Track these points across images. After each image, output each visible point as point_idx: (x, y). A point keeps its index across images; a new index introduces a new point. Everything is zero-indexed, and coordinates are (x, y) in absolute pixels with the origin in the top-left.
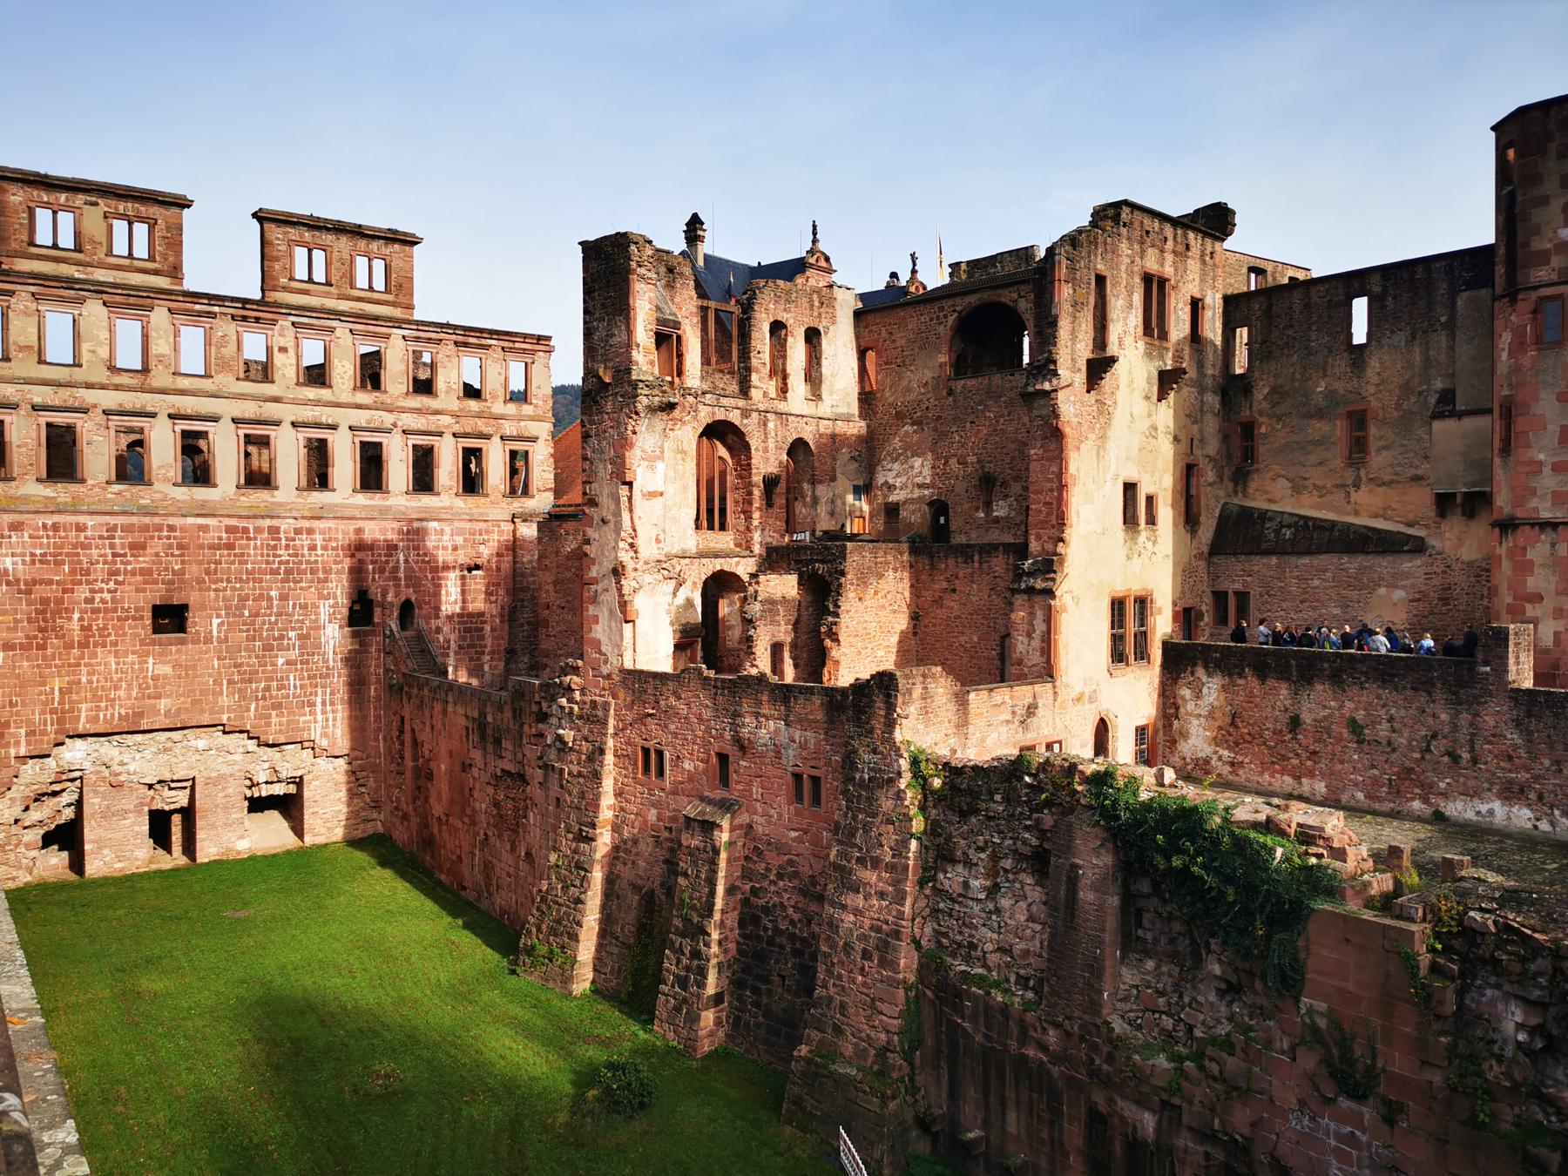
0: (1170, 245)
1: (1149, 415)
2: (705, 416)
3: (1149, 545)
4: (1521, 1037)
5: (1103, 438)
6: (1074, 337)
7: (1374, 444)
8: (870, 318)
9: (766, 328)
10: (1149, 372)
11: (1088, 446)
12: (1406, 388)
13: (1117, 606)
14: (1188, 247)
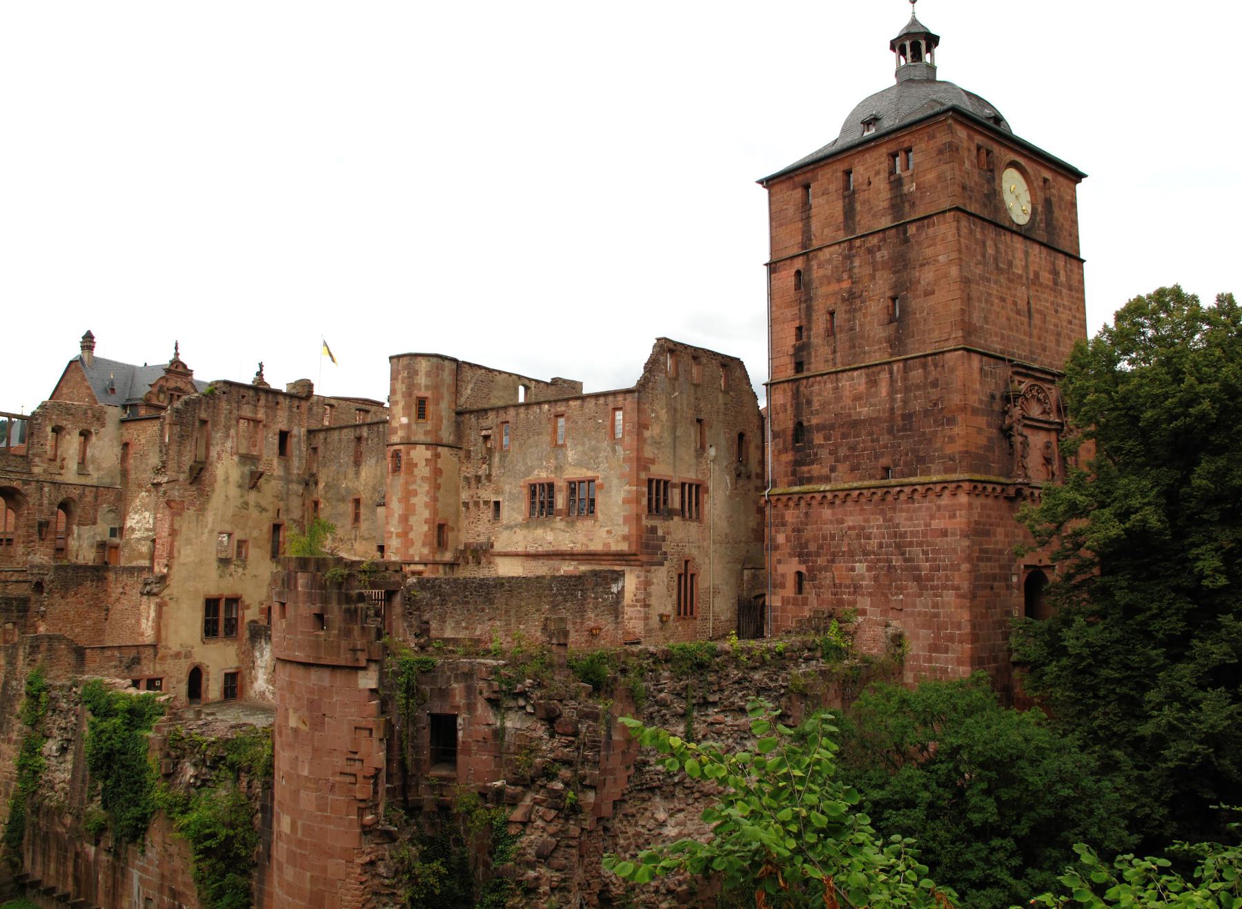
0: (262, 402)
1: (242, 496)
5: (202, 510)
6: (180, 454)
7: (362, 517)
9: (49, 429)
10: (243, 473)
12: (374, 488)
13: (211, 605)
14: (277, 403)
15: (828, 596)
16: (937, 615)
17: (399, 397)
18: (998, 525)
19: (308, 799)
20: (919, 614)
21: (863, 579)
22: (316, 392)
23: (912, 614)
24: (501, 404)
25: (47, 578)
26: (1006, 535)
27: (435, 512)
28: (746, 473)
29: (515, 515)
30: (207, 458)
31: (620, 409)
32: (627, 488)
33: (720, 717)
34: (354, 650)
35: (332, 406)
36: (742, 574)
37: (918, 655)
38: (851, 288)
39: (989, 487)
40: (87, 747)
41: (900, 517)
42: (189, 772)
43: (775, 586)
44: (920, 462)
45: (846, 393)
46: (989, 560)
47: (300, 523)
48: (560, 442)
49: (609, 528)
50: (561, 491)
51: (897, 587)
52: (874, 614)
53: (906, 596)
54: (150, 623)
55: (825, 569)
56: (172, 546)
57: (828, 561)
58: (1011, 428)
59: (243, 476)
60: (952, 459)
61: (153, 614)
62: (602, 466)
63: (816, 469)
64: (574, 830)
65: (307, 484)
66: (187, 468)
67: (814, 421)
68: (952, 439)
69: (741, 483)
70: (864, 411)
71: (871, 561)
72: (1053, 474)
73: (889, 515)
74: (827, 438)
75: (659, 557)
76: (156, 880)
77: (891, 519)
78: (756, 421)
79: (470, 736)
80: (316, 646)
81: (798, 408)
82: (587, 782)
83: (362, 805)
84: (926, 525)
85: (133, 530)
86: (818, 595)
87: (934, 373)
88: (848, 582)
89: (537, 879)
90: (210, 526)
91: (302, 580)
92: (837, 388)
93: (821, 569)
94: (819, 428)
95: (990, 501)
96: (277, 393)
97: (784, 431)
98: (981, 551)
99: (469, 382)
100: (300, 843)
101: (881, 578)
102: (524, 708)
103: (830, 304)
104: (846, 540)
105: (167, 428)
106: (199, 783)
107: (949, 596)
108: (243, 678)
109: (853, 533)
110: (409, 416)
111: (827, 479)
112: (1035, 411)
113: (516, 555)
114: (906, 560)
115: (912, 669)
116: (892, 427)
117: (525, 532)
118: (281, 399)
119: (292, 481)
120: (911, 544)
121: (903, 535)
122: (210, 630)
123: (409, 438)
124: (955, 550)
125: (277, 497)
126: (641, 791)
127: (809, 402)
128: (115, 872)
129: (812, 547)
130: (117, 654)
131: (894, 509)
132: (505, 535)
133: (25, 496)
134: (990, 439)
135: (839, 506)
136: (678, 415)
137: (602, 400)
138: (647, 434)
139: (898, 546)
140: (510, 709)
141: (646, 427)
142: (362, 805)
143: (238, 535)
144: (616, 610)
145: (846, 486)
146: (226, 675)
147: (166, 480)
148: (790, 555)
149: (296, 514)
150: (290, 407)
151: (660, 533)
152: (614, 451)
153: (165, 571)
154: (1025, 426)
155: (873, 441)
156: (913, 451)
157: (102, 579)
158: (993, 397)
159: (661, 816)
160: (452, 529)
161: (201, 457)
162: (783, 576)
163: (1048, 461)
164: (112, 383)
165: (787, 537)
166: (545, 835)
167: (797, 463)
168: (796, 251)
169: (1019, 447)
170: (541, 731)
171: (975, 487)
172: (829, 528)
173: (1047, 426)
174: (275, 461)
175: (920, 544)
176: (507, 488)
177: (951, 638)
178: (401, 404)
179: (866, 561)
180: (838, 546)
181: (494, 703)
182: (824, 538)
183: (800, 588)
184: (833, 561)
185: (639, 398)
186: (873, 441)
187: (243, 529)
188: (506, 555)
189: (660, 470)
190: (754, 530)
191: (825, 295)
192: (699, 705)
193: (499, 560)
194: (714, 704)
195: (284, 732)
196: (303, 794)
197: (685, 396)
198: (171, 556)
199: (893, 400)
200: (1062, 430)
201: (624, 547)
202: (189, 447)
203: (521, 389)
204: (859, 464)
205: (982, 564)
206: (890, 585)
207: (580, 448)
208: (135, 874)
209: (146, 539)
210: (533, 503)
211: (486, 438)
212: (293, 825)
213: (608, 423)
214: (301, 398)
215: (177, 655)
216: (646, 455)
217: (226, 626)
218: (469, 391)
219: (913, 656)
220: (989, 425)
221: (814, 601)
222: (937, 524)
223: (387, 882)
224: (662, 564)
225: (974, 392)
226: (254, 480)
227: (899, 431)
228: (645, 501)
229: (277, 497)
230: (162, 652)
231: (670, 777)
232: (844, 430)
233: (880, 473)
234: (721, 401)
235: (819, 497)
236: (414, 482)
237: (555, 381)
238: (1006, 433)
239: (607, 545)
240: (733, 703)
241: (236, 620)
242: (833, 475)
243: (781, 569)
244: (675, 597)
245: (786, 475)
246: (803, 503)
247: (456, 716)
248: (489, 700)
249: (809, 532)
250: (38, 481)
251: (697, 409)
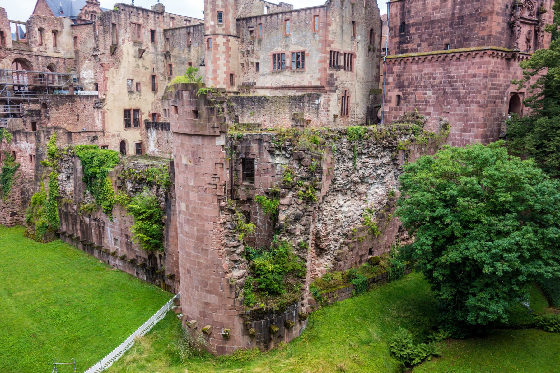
0: (141, 15)
2: (14, 56)
3: (138, 96)
4: (131, 189)
5: (117, 68)
6: (105, 41)
8: (75, 27)
9: (36, 29)
10: (135, 50)
11: (112, 70)
13: (127, 112)
14: (148, 16)
15: (412, 106)
16: (466, 115)
17: (209, 11)
18: (501, 72)
19: (194, 196)
20: (458, 114)
21: (430, 98)
22: (166, 11)
23: (454, 114)
24: (256, 15)
25: (48, 101)
26: (504, 77)
27: (228, 68)
28: (373, 48)
30: (117, 43)
31: (318, 16)
32: (320, 55)
33: (367, 160)
34: (214, 127)
35: (173, 18)
36: (369, 97)
37: (455, 134)
39: (500, 53)
40: (80, 175)
42: (129, 186)
43: (386, 102)
44: (465, 40)
46: (495, 89)
47: (163, 74)
48: (288, 33)
49: (311, 76)
50: (288, 57)
51: (447, 102)
52: (434, 115)
53: (451, 106)
54: (100, 121)
55: (412, 94)
56: (106, 85)
57: (413, 90)
58: (514, 23)
59: (135, 52)
60: (483, 38)
61: (100, 117)
62: (308, 45)
63: (410, 46)
64: (310, 208)
65: (165, 56)
66: (109, 48)
67: (411, 21)
68: (484, 29)
69: (371, 53)
70: (438, 15)
71: (435, 90)
72: (530, 47)
73: (446, 67)
74: (417, 30)
75: (334, 88)
76: (119, 231)
77: (447, 70)
78: (378, 23)
79: (261, 168)
80: (194, 125)
81: (403, 15)
82: (317, 187)
83: (219, 198)
84: (465, 72)
85: (84, 79)
86: (407, 106)
88: (423, 100)
89: (295, 229)
90: (122, 76)
91: (186, 95)
92: (425, 4)
93: (409, 94)
94: (414, 25)
95: (499, 60)
96: (147, 11)
97: (395, 27)
98: (492, 84)
99: (241, 4)
100: (191, 215)
101: (439, 98)
102: (284, 155)
104: (423, 80)
105: (97, 27)
106: (134, 190)
107: (474, 106)
108: (144, 145)
109: (427, 76)
110: (214, 21)
111: (416, 50)
112: (526, 14)
113: (267, 88)
114: (453, 89)
115: (451, 141)
116: (452, 23)
117: (271, 77)
118: (150, 13)
119: (158, 55)
120: (456, 81)
121: (453, 77)
122: (127, 124)
123: (214, 32)
124: (479, 84)
125: (152, 62)
126: (333, 192)
127: (409, 12)
128: (99, 229)
129: (406, 83)
130: (86, 135)
131: (449, 65)
132: (262, 78)
133: (30, 62)
134: (503, 29)
135: (421, 63)
136: (344, 19)
137: (308, 12)
138: (330, 28)
139: (450, 82)
140: (278, 155)
141: (329, 25)
142: (219, 198)
143: (136, 80)
144: (318, 112)
145: (425, 54)
146: (136, 144)
147: (99, 53)
148: (395, 87)
149: (162, 71)
150: (155, 18)
151: (335, 77)
152: (314, 37)
153: (104, 97)
154: (521, 22)
155: (441, 31)
156: (462, 35)
157: (74, 101)
158: (507, 6)
159: (341, 202)
160: (237, 76)
161: (115, 42)
162: (390, 97)
163: (528, 40)
164: (61, 8)
165: (393, 79)
166: (298, 210)
167: (401, 43)
169: (517, 32)
170: (296, 165)
171: (493, 53)
172: (415, 74)
173: (530, 22)
174: (150, 45)
175: (461, 81)
176: (262, 56)
177: (473, 126)
178: (210, 15)
179: (433, 89)
180: (419, 82)
181: (272, 153)
182: (412, 79)
183: (398, 103)
184: (416, 90)
185: (327, 10)
186: (441, 31)
187: (138, 77)
188: (262, 88)
189: (335, 47)
190: (375, 76)
192: (359, 154)
193: (258, 90)
194: (365, 154)
195: (180, 166)
196: (191, 193)
197: (347, 9)
198: (105, 90)
199: (454, 9)
200: (537, 25)
201: (318, 83)
202: (109, 37)
203: (266, 8)
204: (433, 42)
205: (492, 91)
206: (444, 101)
207: (297, 36)
208: (108, 229)
209: (91, 83)
210: (274, 63)
211: (251, 32)
212: (187, 206)
213: (311, 23)
214: (159, 14)
215: (113, 136)
216: (329, 39)
217: (134, 122)
218: (241, 9)
219: (453, 134)
220: (504, 21)
221: (405, 109)
222: (471, 71)
223: (231, 231)
224: (335, 92)
225: (499, 4)
226: (141, 53)
227: (455, 25)
228: (328, 61)
229: (152, 62)
230: (106, 134)
231: (345, 186)
233: (444, 46)
234: (364, 12)
235: (411, 59)
236: (218, 54)
237: (280, 5)
238: (511, 26)
239: (310, 82)
240: (373, 154)
241: (139, 119)
242: (419, 48)
243: (390, 94)
244: (340, 107)
245: (395, 49)
246: (402, 62)
247: (253, 159)
248: (269, 151)
249: (405, 76)
250: (36, 55)
251: (353, 17)
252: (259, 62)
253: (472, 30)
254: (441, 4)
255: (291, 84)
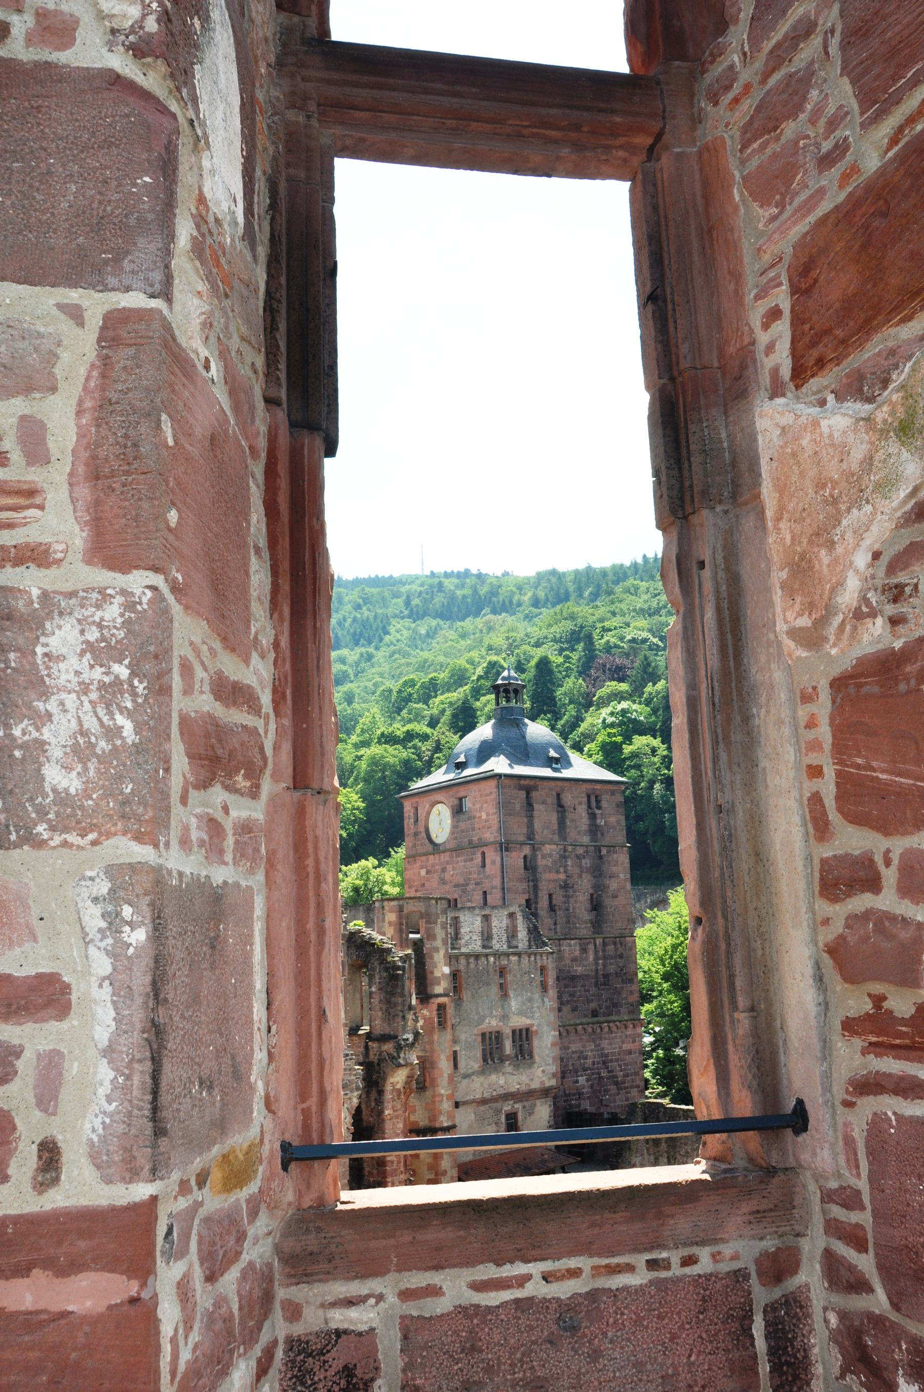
29: (472, 1063)
38: (565, 881)
41: (605, 1043)
45: (566, 955)
68: (631, 993)
70: (579, 970)
77: (599, 1045)
87: (620, 950)
103: (551, 886)
114: (609, 1072)
117: (482, 1079)
120: (611, 1061)
121: (606, 1056)
139: (604, 1063)
152: (543, 1002)
168: (522, 838)
176: (463, 1037)
191: (549, 880)
199: (597, 964)
222: (625, 1047)
232: (566, 982)
252: (458, 1048)
253: (619, 993)
254: (581, 954)
255: (514, 1087)
